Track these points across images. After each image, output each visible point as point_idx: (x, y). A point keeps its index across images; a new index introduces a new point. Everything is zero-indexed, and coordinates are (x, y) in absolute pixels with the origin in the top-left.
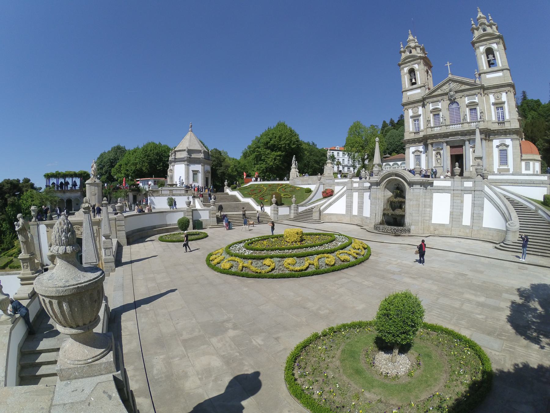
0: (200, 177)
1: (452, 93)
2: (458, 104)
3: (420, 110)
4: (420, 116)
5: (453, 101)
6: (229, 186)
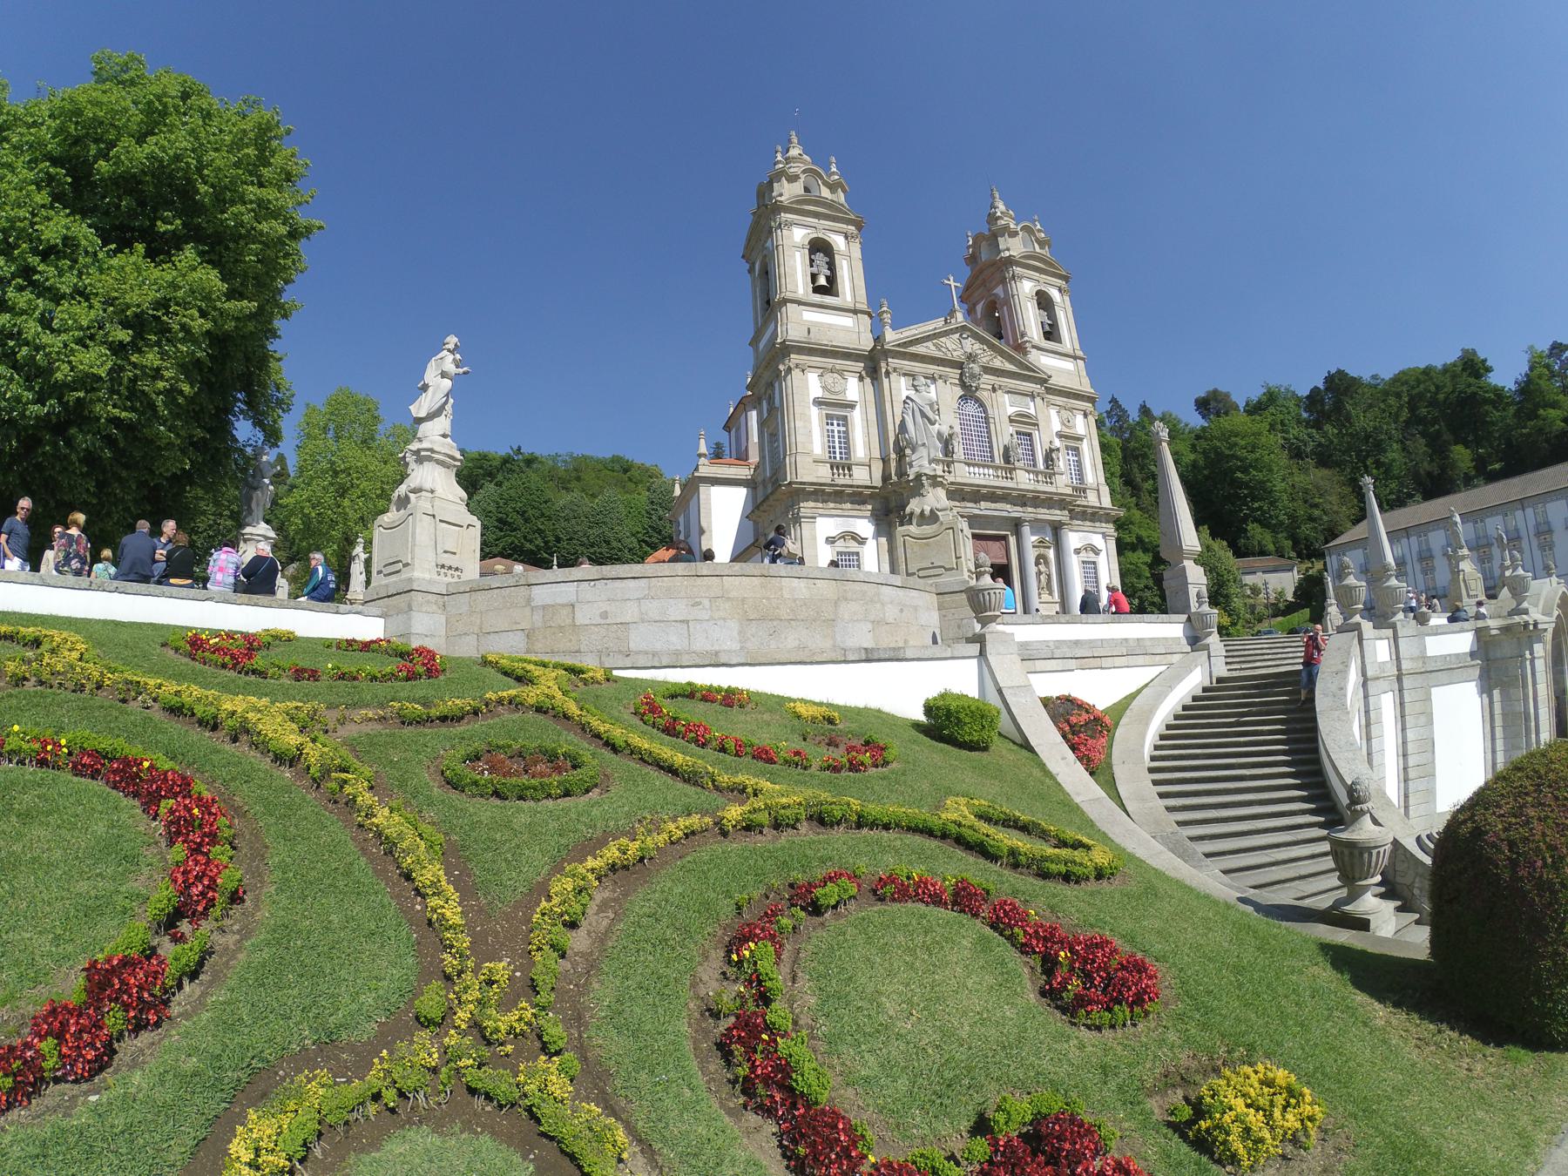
1: (976, 368)
2: (982, 405)
3: (853, 389)
4: (851, 406)
5: (969, 393)
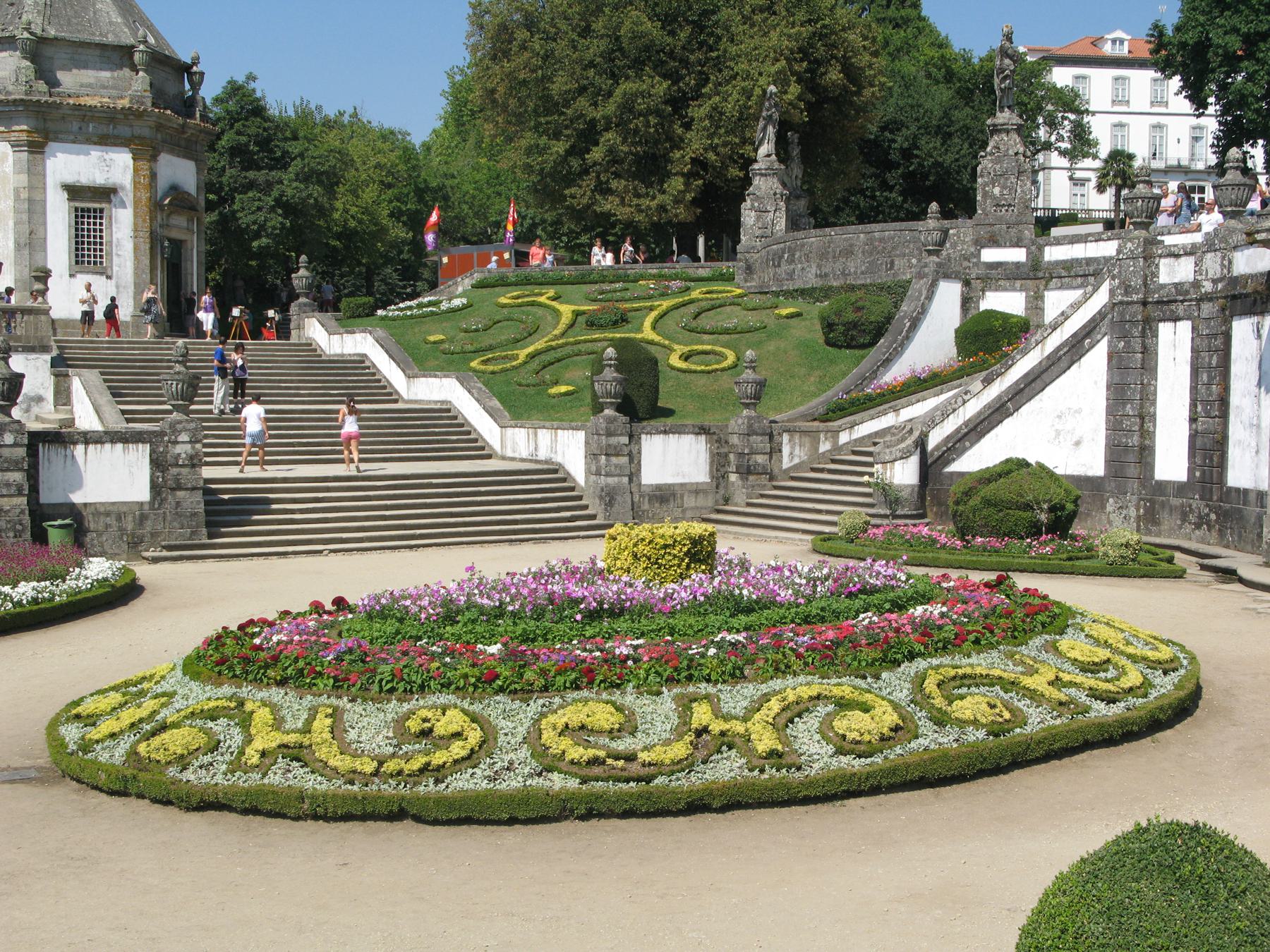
0: (123, 228)
6: (324, 305)
